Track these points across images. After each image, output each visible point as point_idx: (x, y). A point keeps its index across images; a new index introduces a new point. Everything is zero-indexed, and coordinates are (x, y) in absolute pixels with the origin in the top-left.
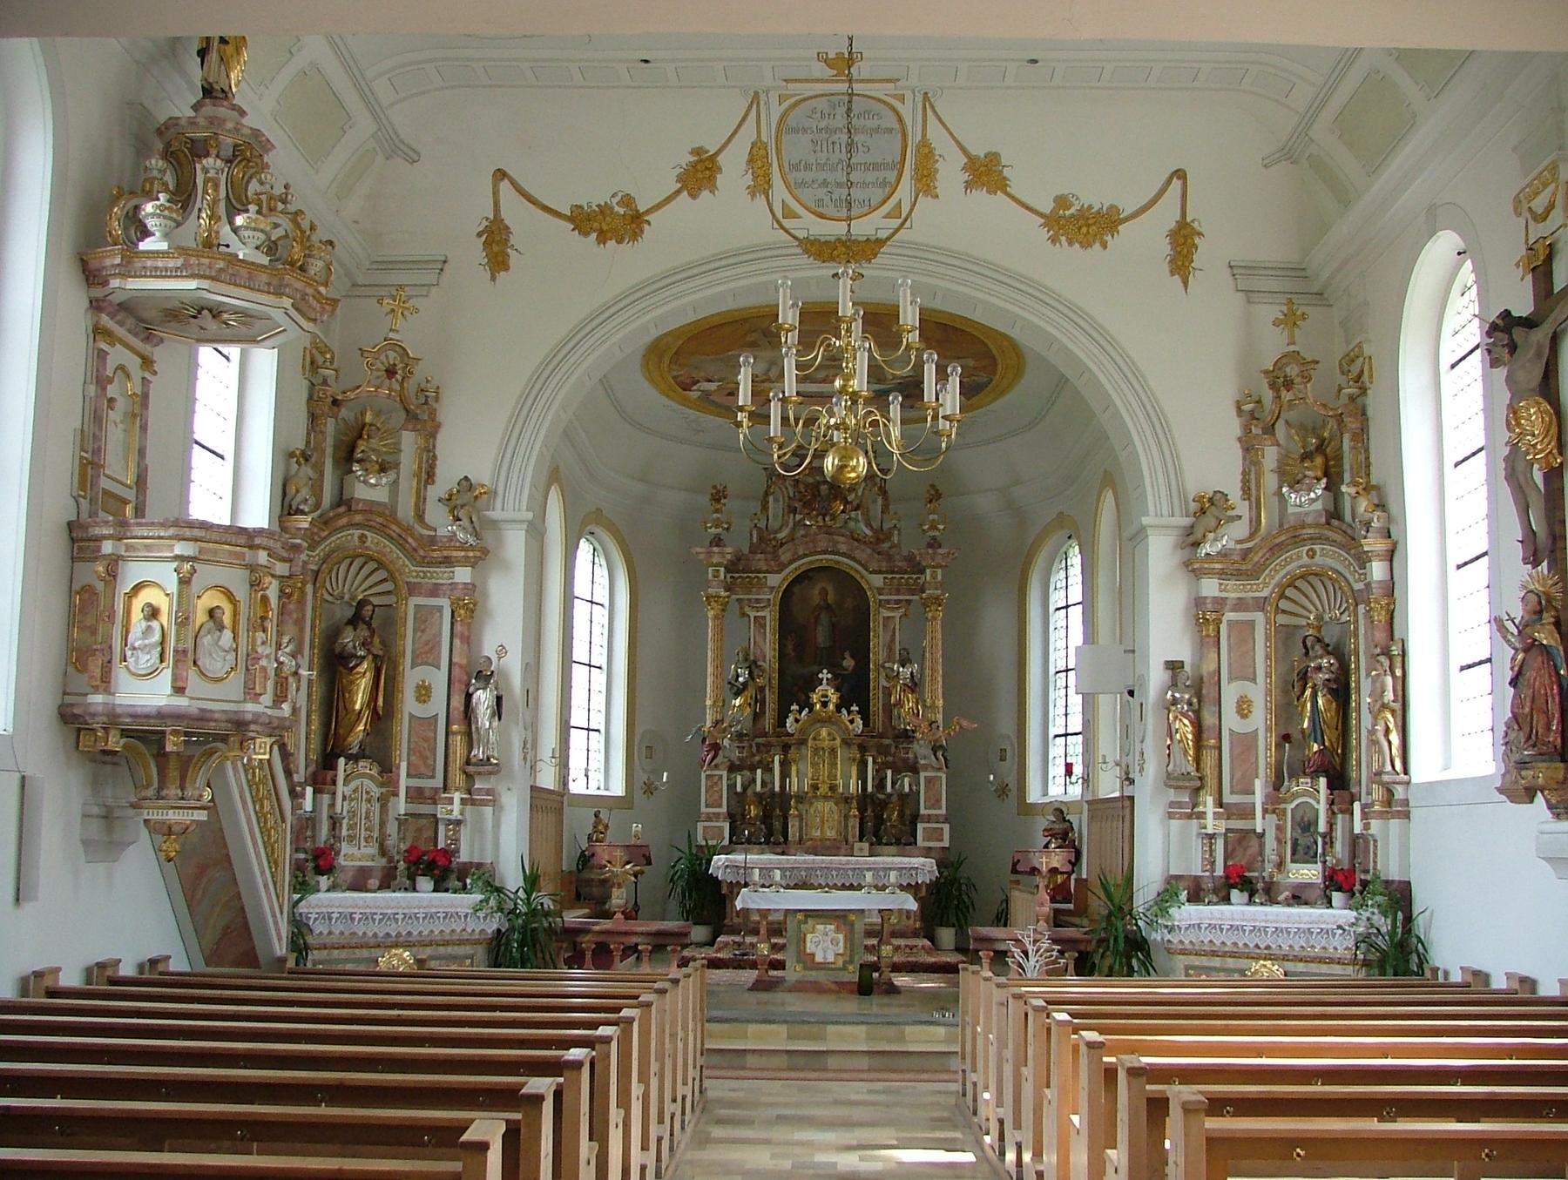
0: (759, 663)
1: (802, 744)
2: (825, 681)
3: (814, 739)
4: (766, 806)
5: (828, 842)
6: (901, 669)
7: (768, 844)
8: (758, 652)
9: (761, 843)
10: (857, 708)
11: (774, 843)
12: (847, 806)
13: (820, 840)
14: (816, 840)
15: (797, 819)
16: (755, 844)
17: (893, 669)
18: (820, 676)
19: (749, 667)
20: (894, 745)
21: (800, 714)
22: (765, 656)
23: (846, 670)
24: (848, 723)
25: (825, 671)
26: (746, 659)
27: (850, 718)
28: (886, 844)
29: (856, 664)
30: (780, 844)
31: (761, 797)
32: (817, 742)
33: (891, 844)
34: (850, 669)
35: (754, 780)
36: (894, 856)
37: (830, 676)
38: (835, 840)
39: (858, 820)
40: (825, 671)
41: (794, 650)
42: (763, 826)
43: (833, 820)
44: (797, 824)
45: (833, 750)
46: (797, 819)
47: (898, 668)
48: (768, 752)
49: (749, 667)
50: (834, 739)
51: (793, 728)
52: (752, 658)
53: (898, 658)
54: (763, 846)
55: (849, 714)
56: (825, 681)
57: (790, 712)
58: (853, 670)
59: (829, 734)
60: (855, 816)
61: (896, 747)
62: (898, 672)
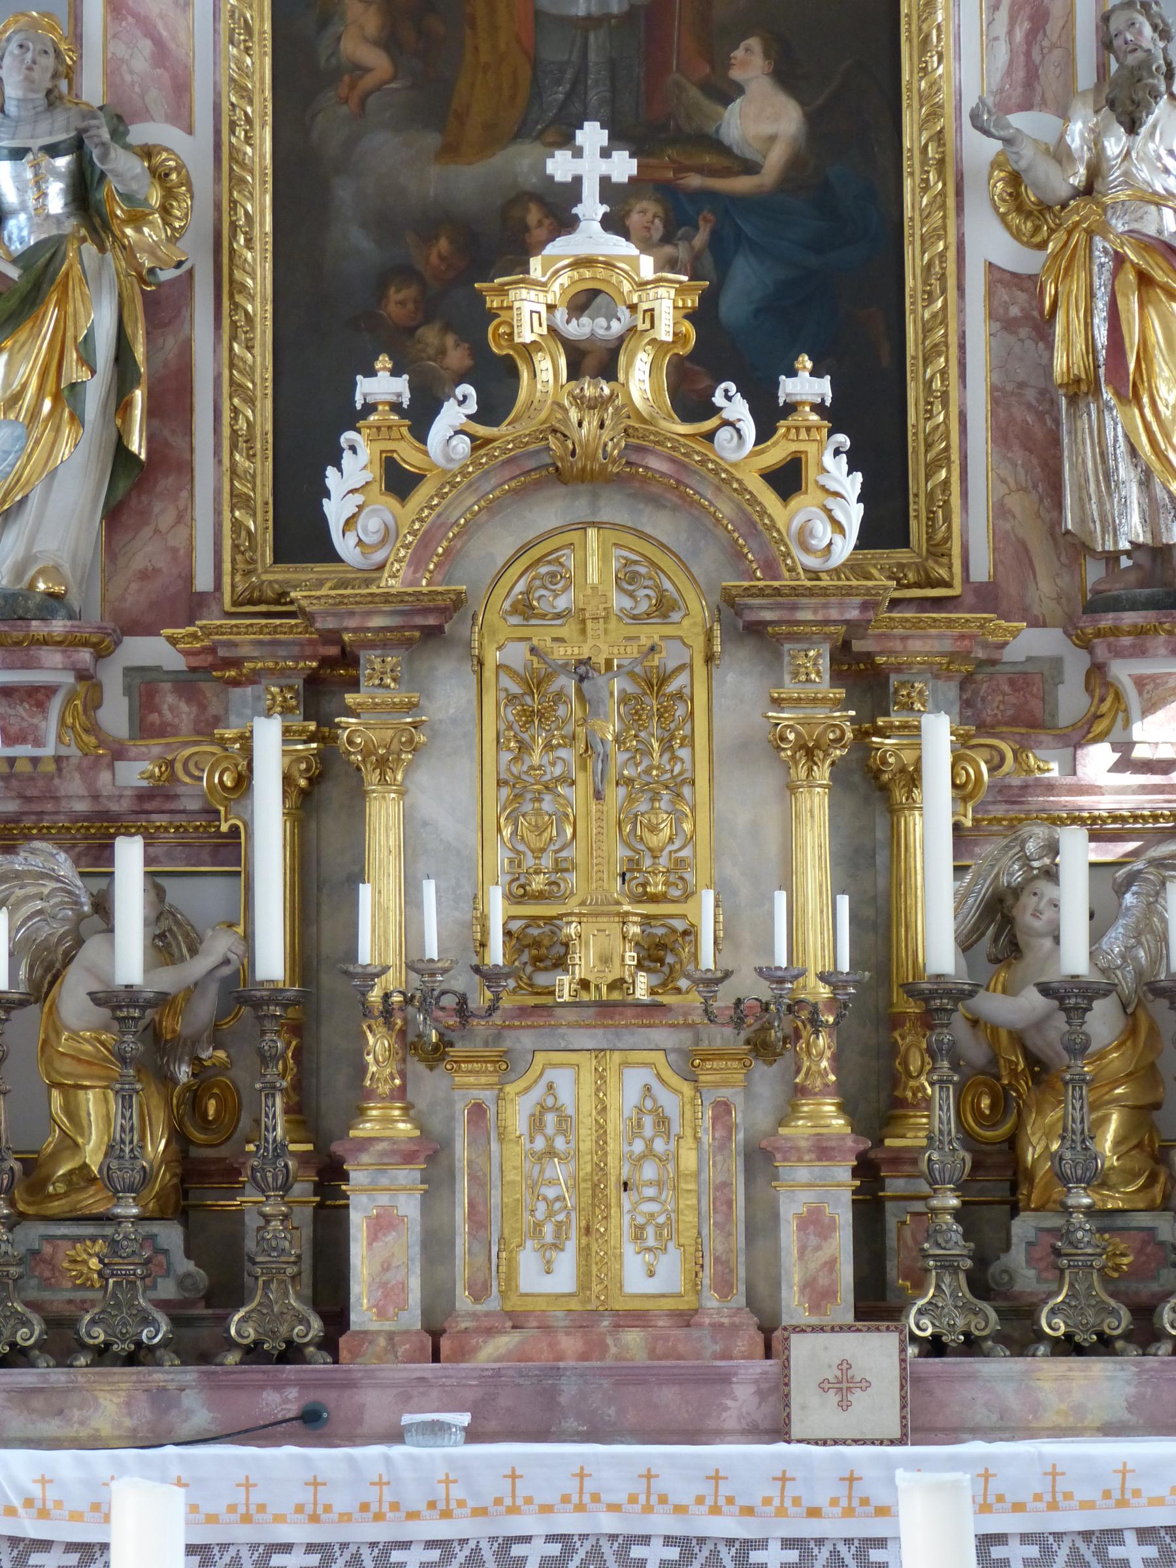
0: (139, 133)
1: (433, 634)
2: (591, 209)
3: (525, 609)
4: (195, 1098)
5: (633, 1338)
6: (1114, 146)
7: (203, 1357)
8: (140, 60)
9: (139, 1355)
10: (823, 388)
11: (254, 1353)
12: (767, 1078)
13: (585, 1322)
14: (546, 1328)
15: (408, 1175)
16: (102, 1355)
17: (1061, 155)
18: (560, 167)
19: (78, 146)
20: (1076, 665)
21: (420, 432)
22: (181, 88)
23: (750, 168)
24: (768, 498)
25: (592, 135)
26: (52, 99)
27: (776, 453)
28: (1068, 1347)
29: (813, 119)
30: (291, 1353)
31: (154, 1033)
32: (542, 636)
33: (1104, 1346)
34: (775, 160)
35: (103, 907)
36: (1112, 1430)
37: (623, 166)
38: (685, 1319)
39: (843, 1172)
40: (592, 135)
41: (389, 43)
42: (171, 1235)
43: (670, 1183)
44: (409, 1207)
45: (655, 682)
46: (408, 1175)
47: (1096, 140)
48: (206, 728)
49: (78, 146)
50: (664, 608)
51: (371, 526)
52: (93, 90)
53: (1086, 76)
54: (158, 1376)
55: (764, 434)
56: (591, 209)
57: (353, 417)
58: (795, 164)
59: (628, 579)
60: (823, 1150)
61: (1097, 673)
62: (1096, 171)
